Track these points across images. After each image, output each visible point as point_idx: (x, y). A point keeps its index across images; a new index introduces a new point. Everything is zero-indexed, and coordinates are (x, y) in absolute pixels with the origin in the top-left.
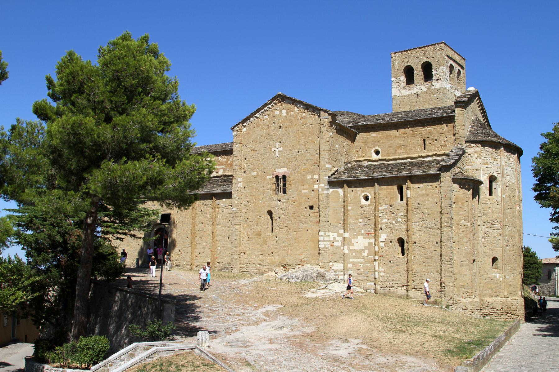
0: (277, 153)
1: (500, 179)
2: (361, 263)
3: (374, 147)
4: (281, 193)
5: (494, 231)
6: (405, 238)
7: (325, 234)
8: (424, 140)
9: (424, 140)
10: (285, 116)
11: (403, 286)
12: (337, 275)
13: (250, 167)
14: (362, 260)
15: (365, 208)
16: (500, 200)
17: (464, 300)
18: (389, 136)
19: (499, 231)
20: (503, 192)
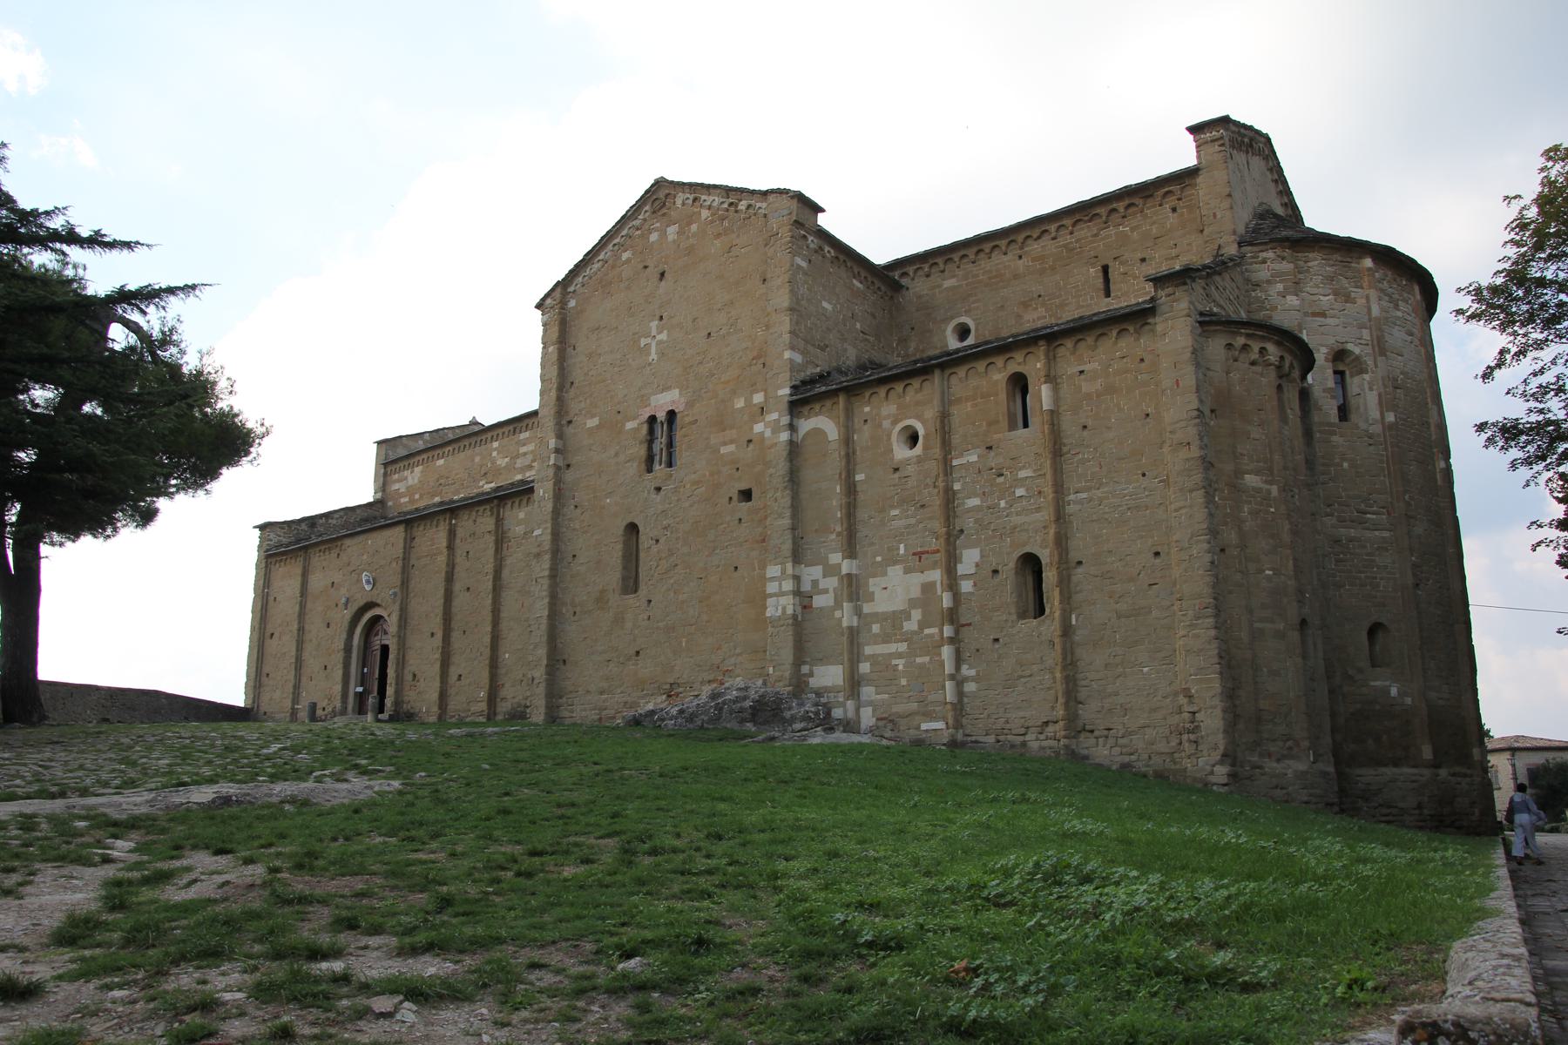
0: (653, 350)
1: (1370, 363)
2: (900, 655)
3: (952, 318)
4: (663, 466)
5: (1368, 534)
6: (1045, 556)
7: (783, 572)
8: (1105, 269)
9: (1105, 269)
10: (674, 241)
11: (1046, 723)
12: (824, 705)
13: (583, 405)
14: (902, 647)
15: (910, 470)
16: (1376, 429)
17: (1275, 765)
18: (996, 277)
19: (1386, 534)
20: (1385, 405)
